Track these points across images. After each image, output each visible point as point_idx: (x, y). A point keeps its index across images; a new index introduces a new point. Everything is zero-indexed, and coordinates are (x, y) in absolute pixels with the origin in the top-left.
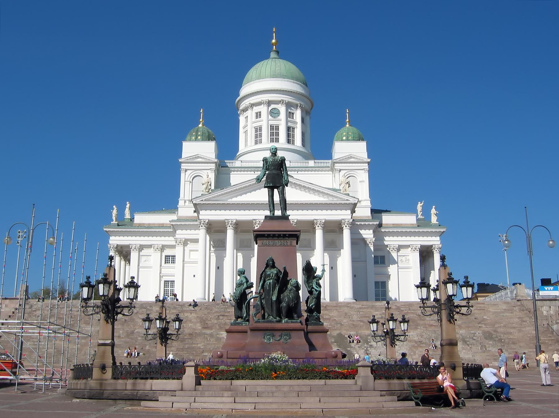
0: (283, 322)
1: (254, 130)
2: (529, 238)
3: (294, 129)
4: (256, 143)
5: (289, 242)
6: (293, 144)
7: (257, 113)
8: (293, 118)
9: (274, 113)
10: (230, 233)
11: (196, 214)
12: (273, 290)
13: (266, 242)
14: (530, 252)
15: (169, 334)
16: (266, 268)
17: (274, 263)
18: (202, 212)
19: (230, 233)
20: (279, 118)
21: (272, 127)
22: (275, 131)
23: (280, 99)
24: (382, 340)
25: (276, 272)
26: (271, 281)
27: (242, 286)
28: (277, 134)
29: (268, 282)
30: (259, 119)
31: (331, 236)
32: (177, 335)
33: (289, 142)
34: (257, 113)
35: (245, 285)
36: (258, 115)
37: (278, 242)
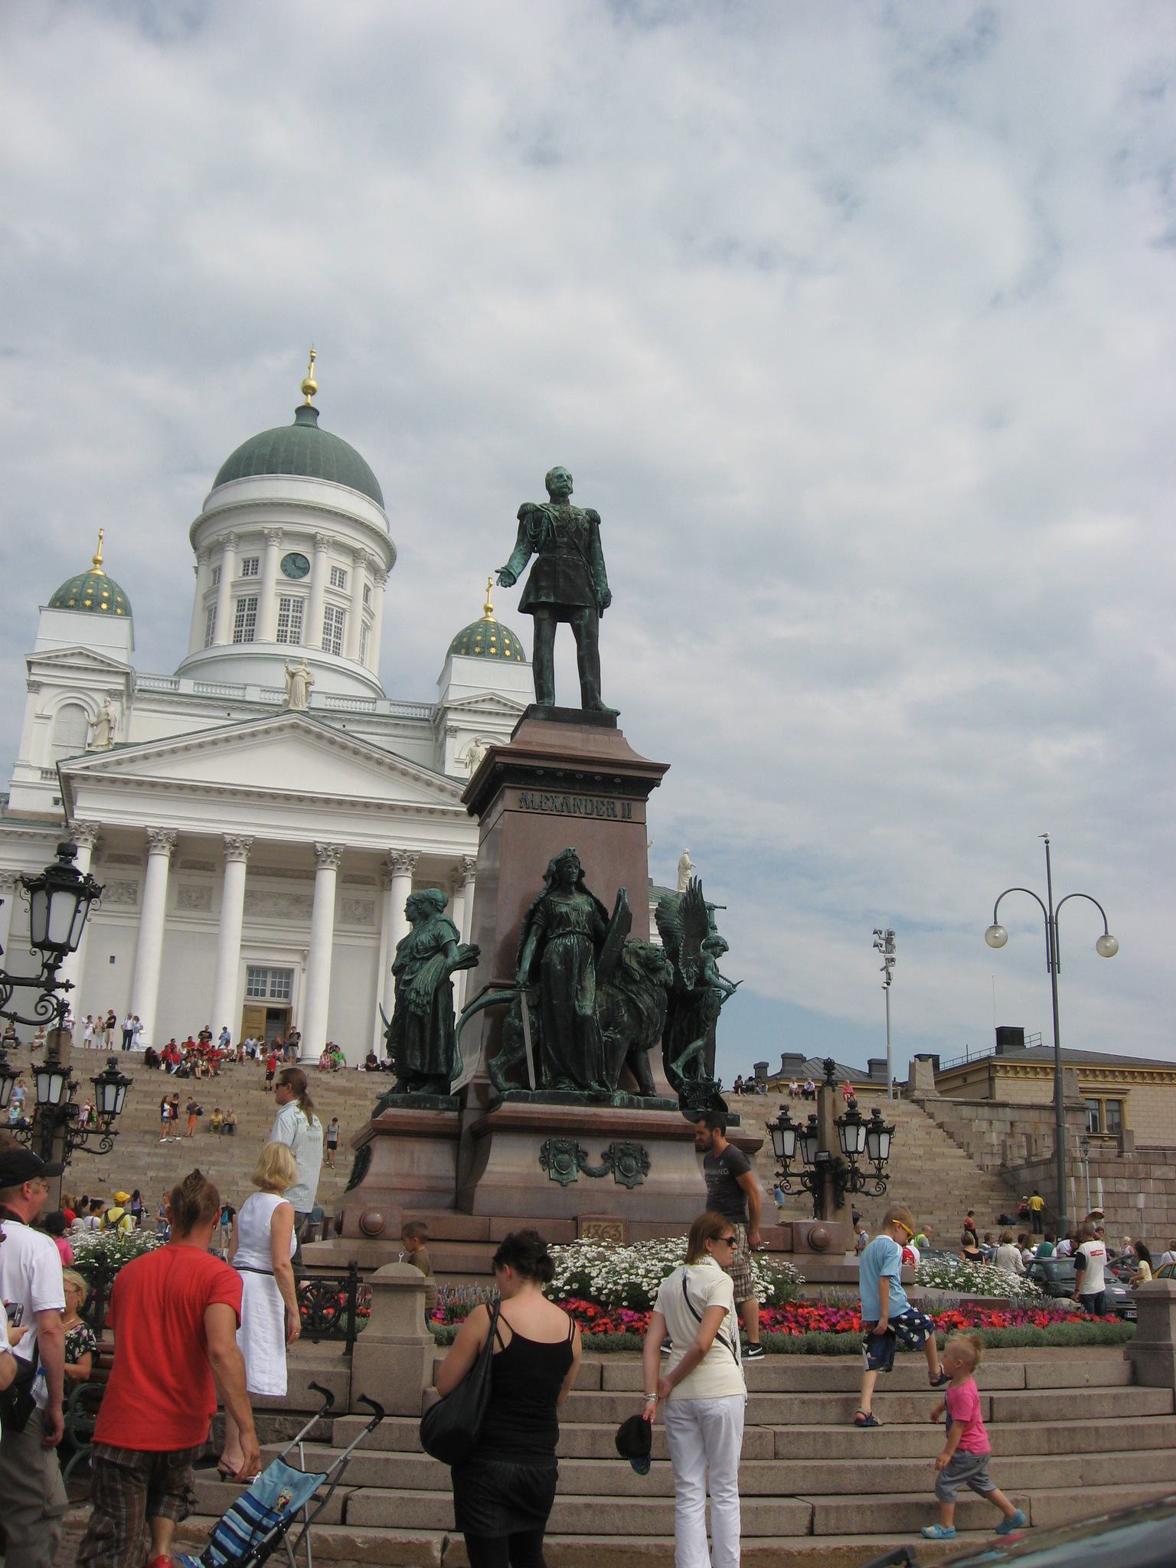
0: (617, 1101)
1: (235, 604)
2: (1051, 923)
3: (341, 613)
4: (237, 640)
5: (618, 804)
9: (297, 566)
10: (160, 865)
11: (60, 810)
12: (580, 982)
13: (537, 797)
14: (1053, 964)
15: (77, 1132)
16: (550, 890)
17: (582, 874)
18: (82, 801)
19: (160, 865)
20: (306, 579)
21: (284, 603)
22: (291, 613)
24: (809, 1189)
25: (588, 908)
26: (571, 941)
27: (439, 957)
28: (298, 621)
29: (558, 945)
32: (107, 1133)
33: (325, 647)
34: (246, 562)
35: (455, 955)
36: (251, 566)
37: (583, 802)
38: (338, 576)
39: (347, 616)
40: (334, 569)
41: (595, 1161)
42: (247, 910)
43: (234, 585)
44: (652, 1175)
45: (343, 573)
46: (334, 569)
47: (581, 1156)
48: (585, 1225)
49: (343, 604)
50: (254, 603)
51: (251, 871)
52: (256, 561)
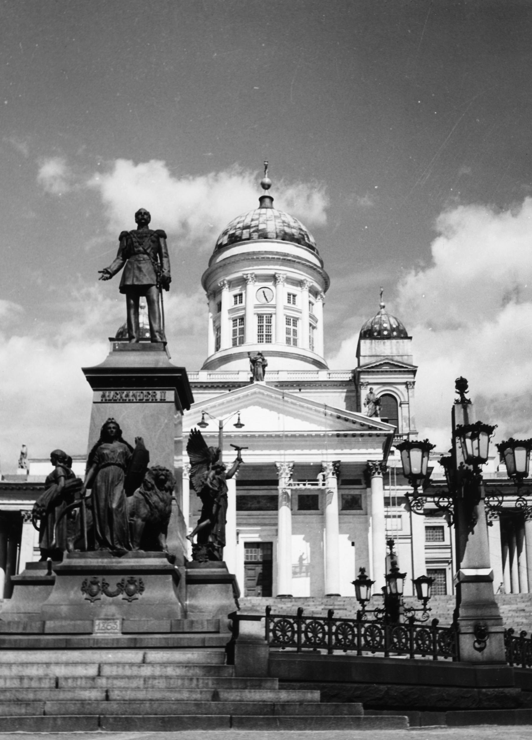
3: (295, 320)
4: (234, 344)
5: (158, 393)
6: (295, 344)
7: (235, 296)
8: (294, 303)
17: (119, 432)
23: (272, 272)
30: (239, 305)
31: (354, 491)
34: (235, 296)
36: (239, 297)
38: (291, 297)
39: (299, 323)
40: (289, 294)
41: (112, 588)
42: (239, 508)
43: (231, 311)
44: (144, 593)
45: (294, 296)
46: (289, 294)
47: (105, 585)
48: (97, 622)
49: (296, 315)
50: (242, 319)
51: (239, 483)
52: (241, 295)
